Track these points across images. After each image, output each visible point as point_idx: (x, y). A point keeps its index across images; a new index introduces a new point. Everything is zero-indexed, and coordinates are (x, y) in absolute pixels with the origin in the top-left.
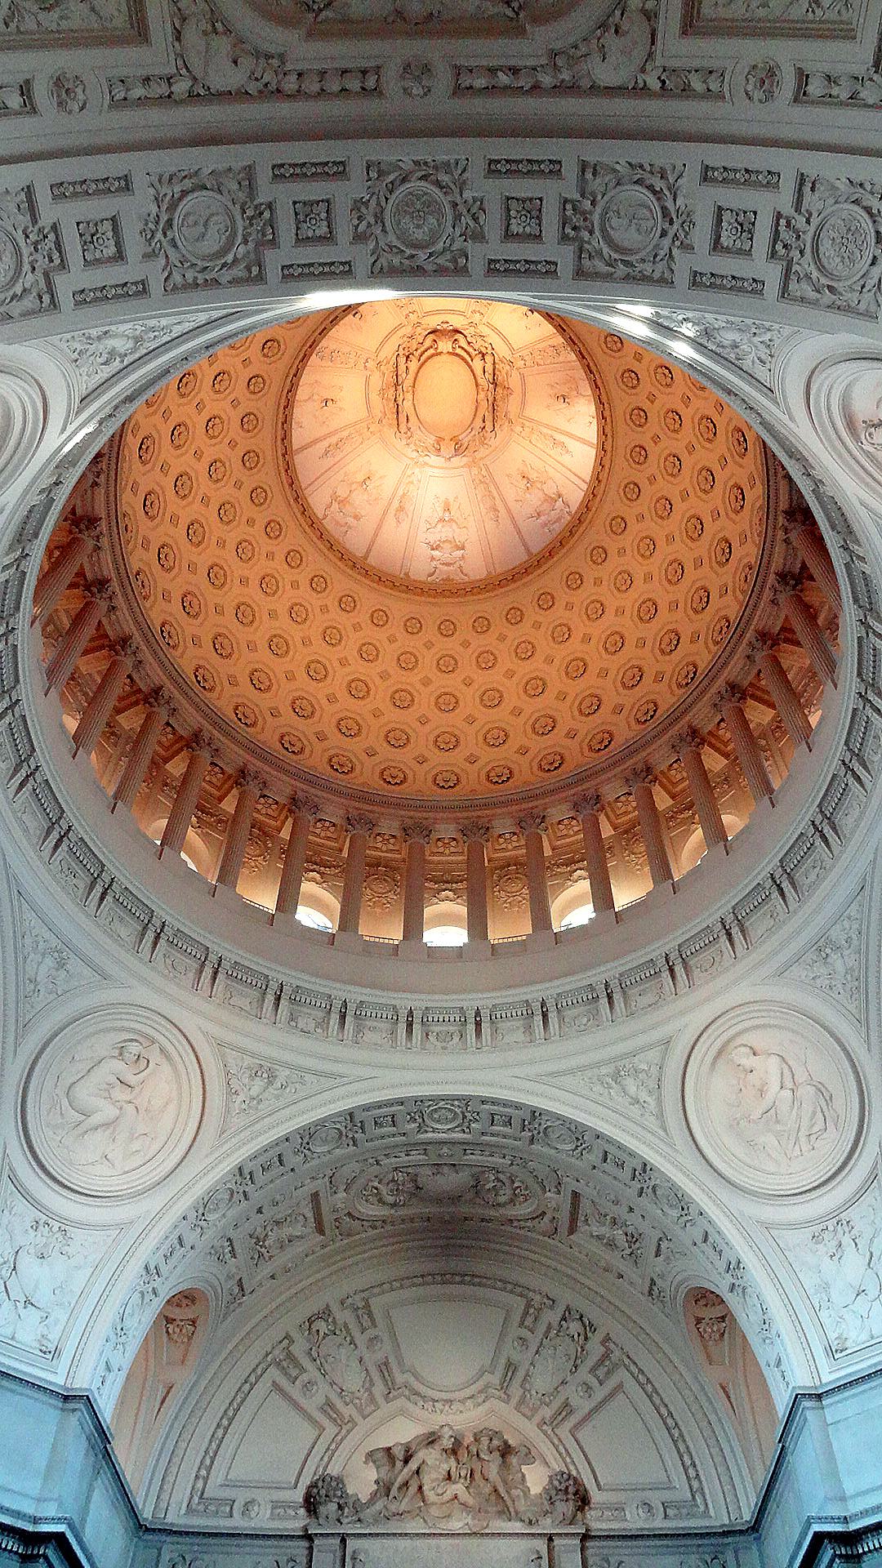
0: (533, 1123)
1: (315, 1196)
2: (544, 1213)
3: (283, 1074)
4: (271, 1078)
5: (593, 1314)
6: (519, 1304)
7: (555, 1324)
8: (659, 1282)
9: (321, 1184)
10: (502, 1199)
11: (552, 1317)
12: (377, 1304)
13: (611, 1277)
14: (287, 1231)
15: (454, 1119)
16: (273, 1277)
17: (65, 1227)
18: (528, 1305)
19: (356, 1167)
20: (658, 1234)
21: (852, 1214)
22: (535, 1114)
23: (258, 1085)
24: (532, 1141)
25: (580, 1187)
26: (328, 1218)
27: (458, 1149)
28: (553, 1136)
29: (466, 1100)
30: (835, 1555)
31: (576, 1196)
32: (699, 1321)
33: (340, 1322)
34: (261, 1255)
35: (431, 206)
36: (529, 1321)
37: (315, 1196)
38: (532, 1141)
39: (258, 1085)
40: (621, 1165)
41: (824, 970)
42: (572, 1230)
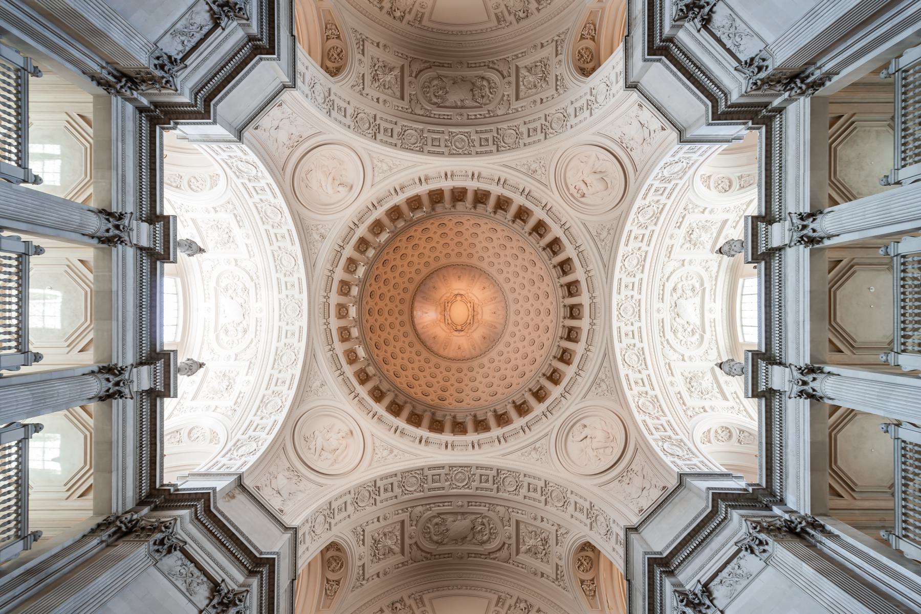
0: (498, 476)
1: (403, 522)
2: (504, 544)
3: (396, 452)
4: (391, 452)
5: (531, 600)
6: (495, 597)
7: (513, 604)
8: (560, 563)
9: (404, 516)
10: (485, 538)
11: (513, 602)
12: (426, 598)
13: (538, 578)
14: (389, 542)
15: (464, 480)
16: (378, 575)
17: (299, 476)
18: (499, 598)
19: (420, 509)
20: (555, 528)
21: (633, 466)
22: (499, 471)
23: (386, 453)
24: (498, 490)
25: (520, 517)
26: (407, 541)
27: (465, 500)
28: (506, 484)
29: (469, 467)
30: (661, 572)
31: (518, 522)
32: (582, 582)
33: (408, 604)
34: (375, 555)
35: (463, 140)
36: (500, 604)
37: (403, 522)
38: (498, 490)
39: (386, 453)
40: (535, 490)
41: (600, 390)
42: (518, 553)
